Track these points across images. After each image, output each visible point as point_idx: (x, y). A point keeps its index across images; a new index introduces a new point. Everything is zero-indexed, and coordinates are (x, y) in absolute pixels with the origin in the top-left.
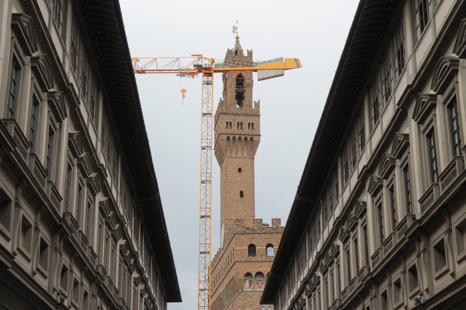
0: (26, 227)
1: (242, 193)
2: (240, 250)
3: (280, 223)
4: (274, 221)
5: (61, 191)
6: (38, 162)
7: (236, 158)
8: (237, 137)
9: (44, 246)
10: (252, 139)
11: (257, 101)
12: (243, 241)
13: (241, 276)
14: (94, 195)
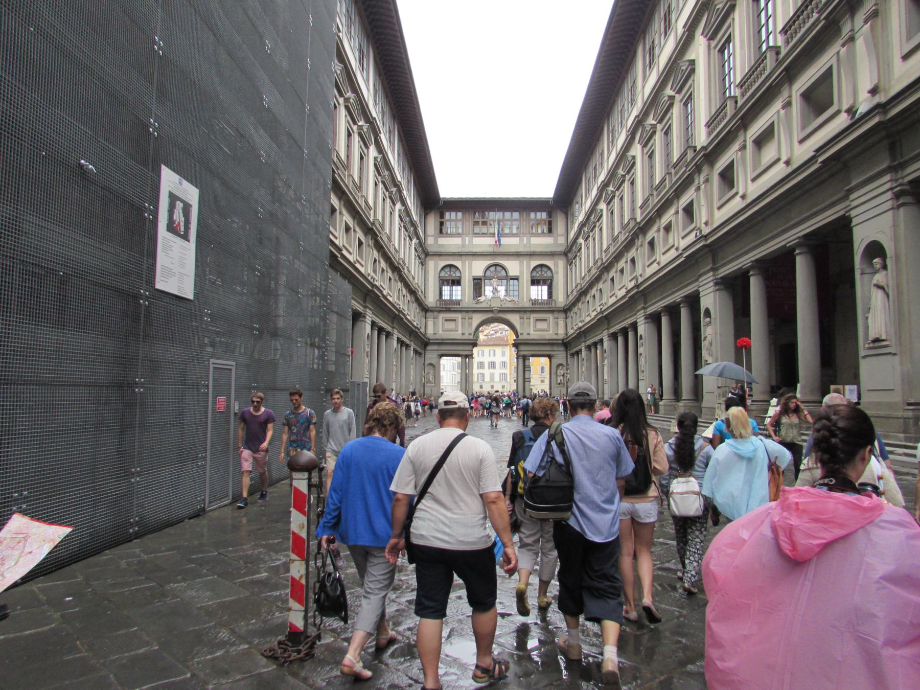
0: (348, 229)
5: (371, 203)
6: (353, 181)
9: (360, 243)
14: (394, 204)
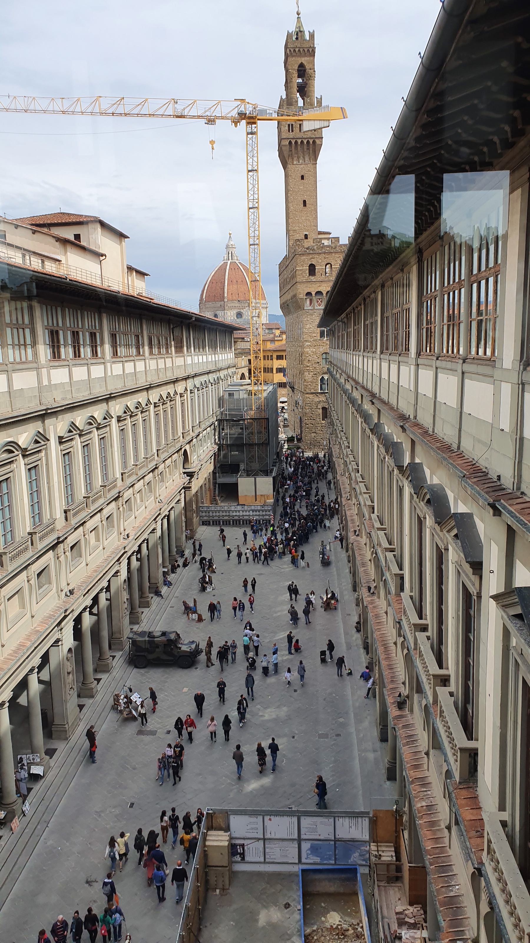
1: (305, 202)
2: (301, 270)
3: (339, 242)
4: (333, 240)
7: (299, 167)
8: (299, 141)
10: (314, 142)
11: (319, 97)
12: (304, 261)
13: (302, 296)
